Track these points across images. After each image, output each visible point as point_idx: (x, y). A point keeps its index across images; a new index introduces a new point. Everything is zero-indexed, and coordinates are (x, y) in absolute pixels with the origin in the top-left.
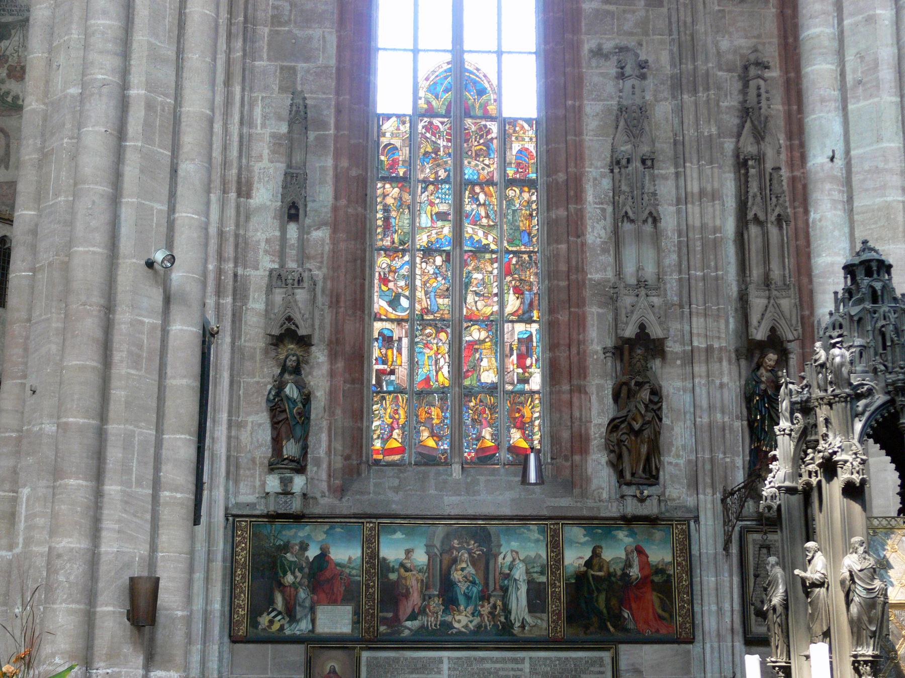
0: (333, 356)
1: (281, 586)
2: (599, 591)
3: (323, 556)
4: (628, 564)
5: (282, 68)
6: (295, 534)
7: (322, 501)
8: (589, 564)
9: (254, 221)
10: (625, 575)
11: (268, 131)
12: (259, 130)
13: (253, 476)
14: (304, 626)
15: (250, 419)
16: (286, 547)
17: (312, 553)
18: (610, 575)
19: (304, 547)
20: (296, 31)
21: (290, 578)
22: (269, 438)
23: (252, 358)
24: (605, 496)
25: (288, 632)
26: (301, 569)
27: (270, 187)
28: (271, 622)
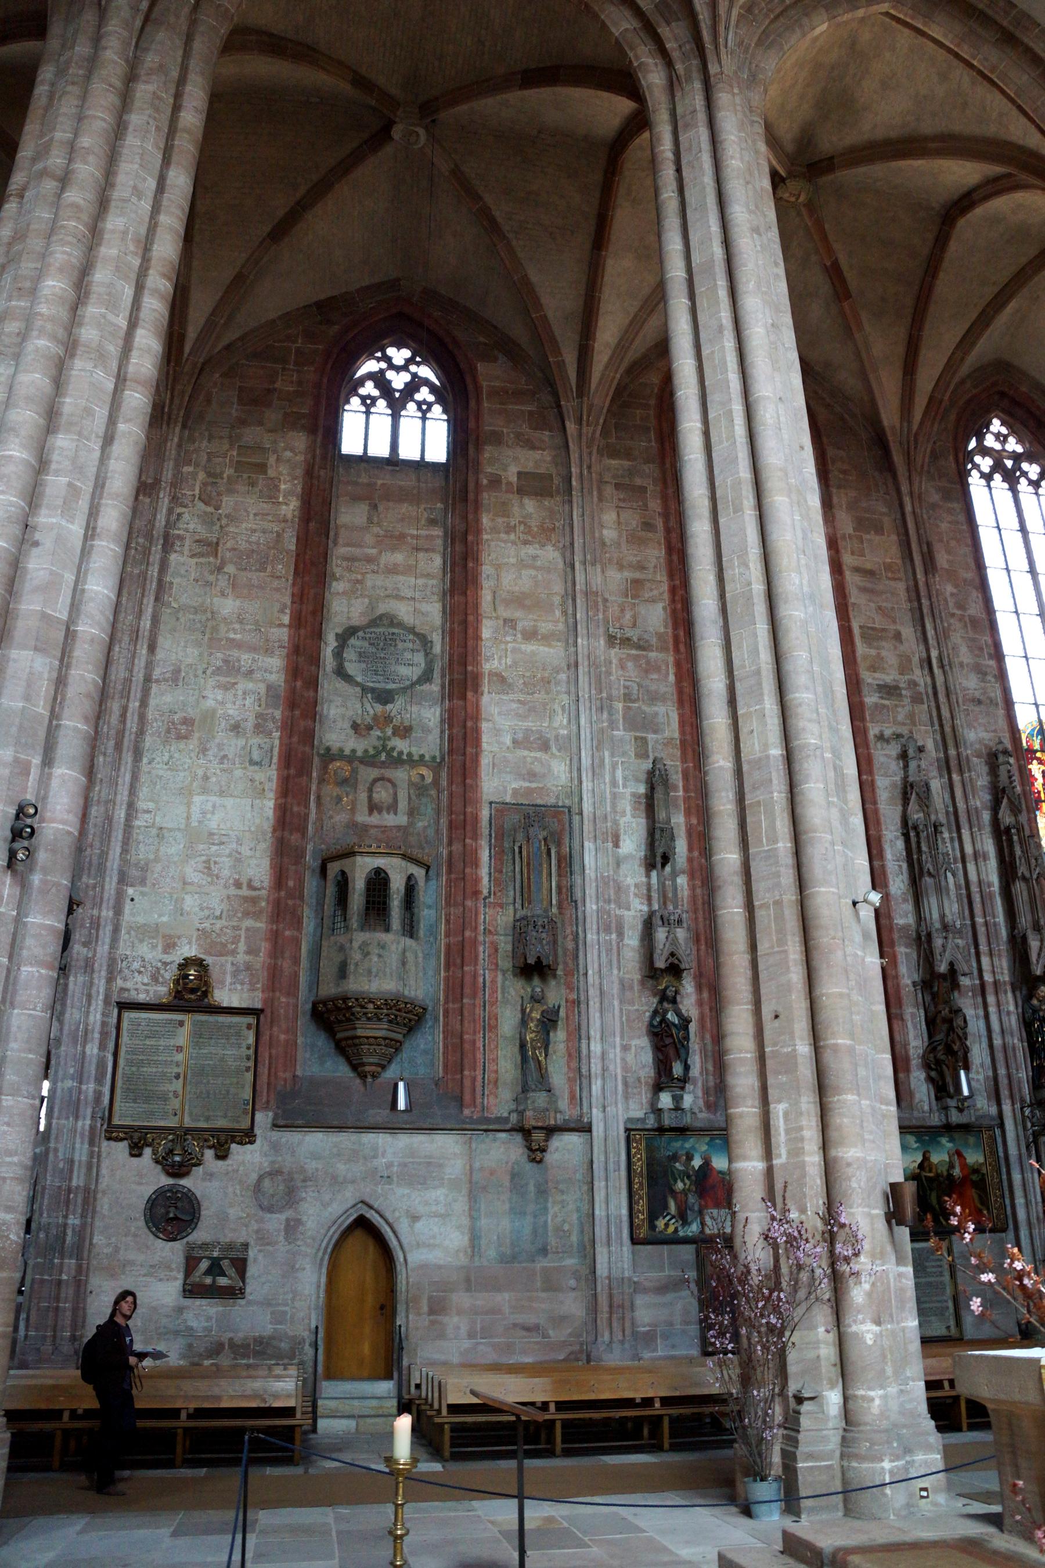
0: (699, 988)
1: (673, 1192)
2: (931, 1190)
3: (707, 1164)
4: (951, 1166)
5: (636, 738)
6: (678, 1145)
7: (700, 1116)
8: (921, 1166)
9: (624, 867)
10: (950, 1176)
11: (629, 790)
12: (621, 790)
13: (640, 1093)
14: (694, 1228)
15: (634, 1042)
16: (675, 1158)
17: (697, 1163)
18: (938, 1175)
19: (690, 1158)
20: (645, 708)
21: (680, 1185)
22: (651, 1060)
23: (631, 988)
24: (926, 1108)
25: (681, 1234)
26: (689, 1177)
27: (634, 839)
28: (667, 1225)
